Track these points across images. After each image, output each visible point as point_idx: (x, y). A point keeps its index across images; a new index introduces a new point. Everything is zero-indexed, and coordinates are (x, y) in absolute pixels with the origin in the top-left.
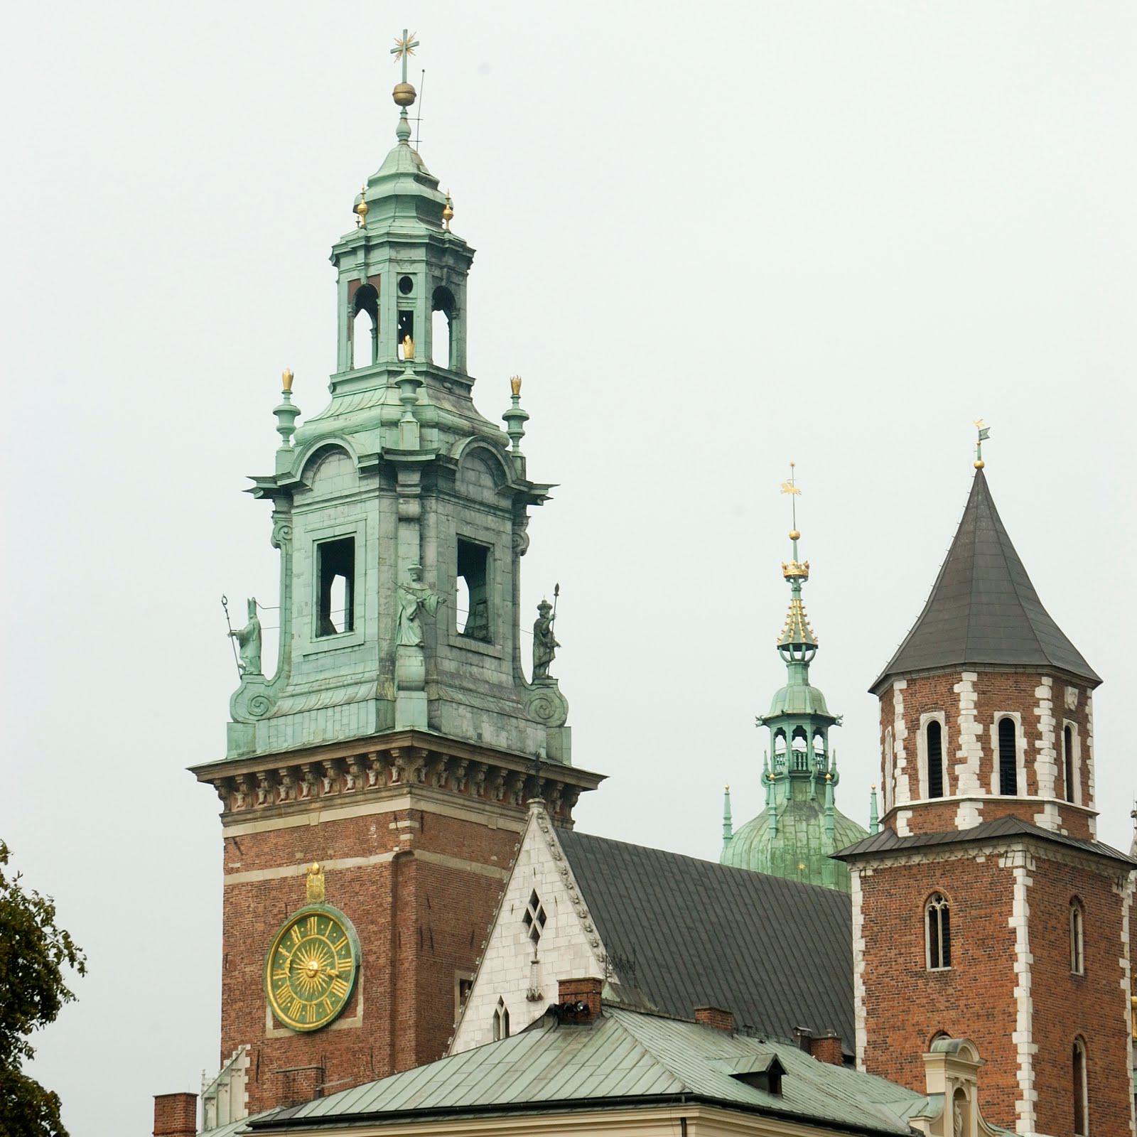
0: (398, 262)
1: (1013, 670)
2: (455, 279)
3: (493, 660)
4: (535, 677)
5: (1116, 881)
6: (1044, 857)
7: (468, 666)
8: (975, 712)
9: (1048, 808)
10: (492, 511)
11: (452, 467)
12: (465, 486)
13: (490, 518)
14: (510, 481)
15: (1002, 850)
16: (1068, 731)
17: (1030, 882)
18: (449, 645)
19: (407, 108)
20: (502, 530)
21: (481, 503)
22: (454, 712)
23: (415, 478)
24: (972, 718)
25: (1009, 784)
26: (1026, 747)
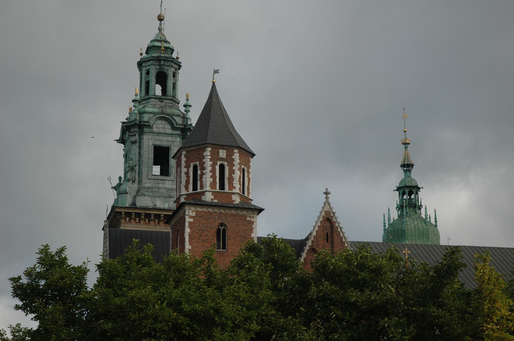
0: (145, 66)
1: (196, 148)
2: (165, 67)
3: (170, 181)
5: (250, 215)
7: (158, 185)
8: (185, 165)
9: (205, 193)
10: (170, 135)
11: (147, 124)
12: (158, 129)
13: (169, 138)
14: (175, 125)
16: (222, 167)
17: (191, 220)
19: (162, 22)
20: (175, 140)
21: (166, 134)
24: (184, 167)
25: (195, 188)
26: (200, 173)
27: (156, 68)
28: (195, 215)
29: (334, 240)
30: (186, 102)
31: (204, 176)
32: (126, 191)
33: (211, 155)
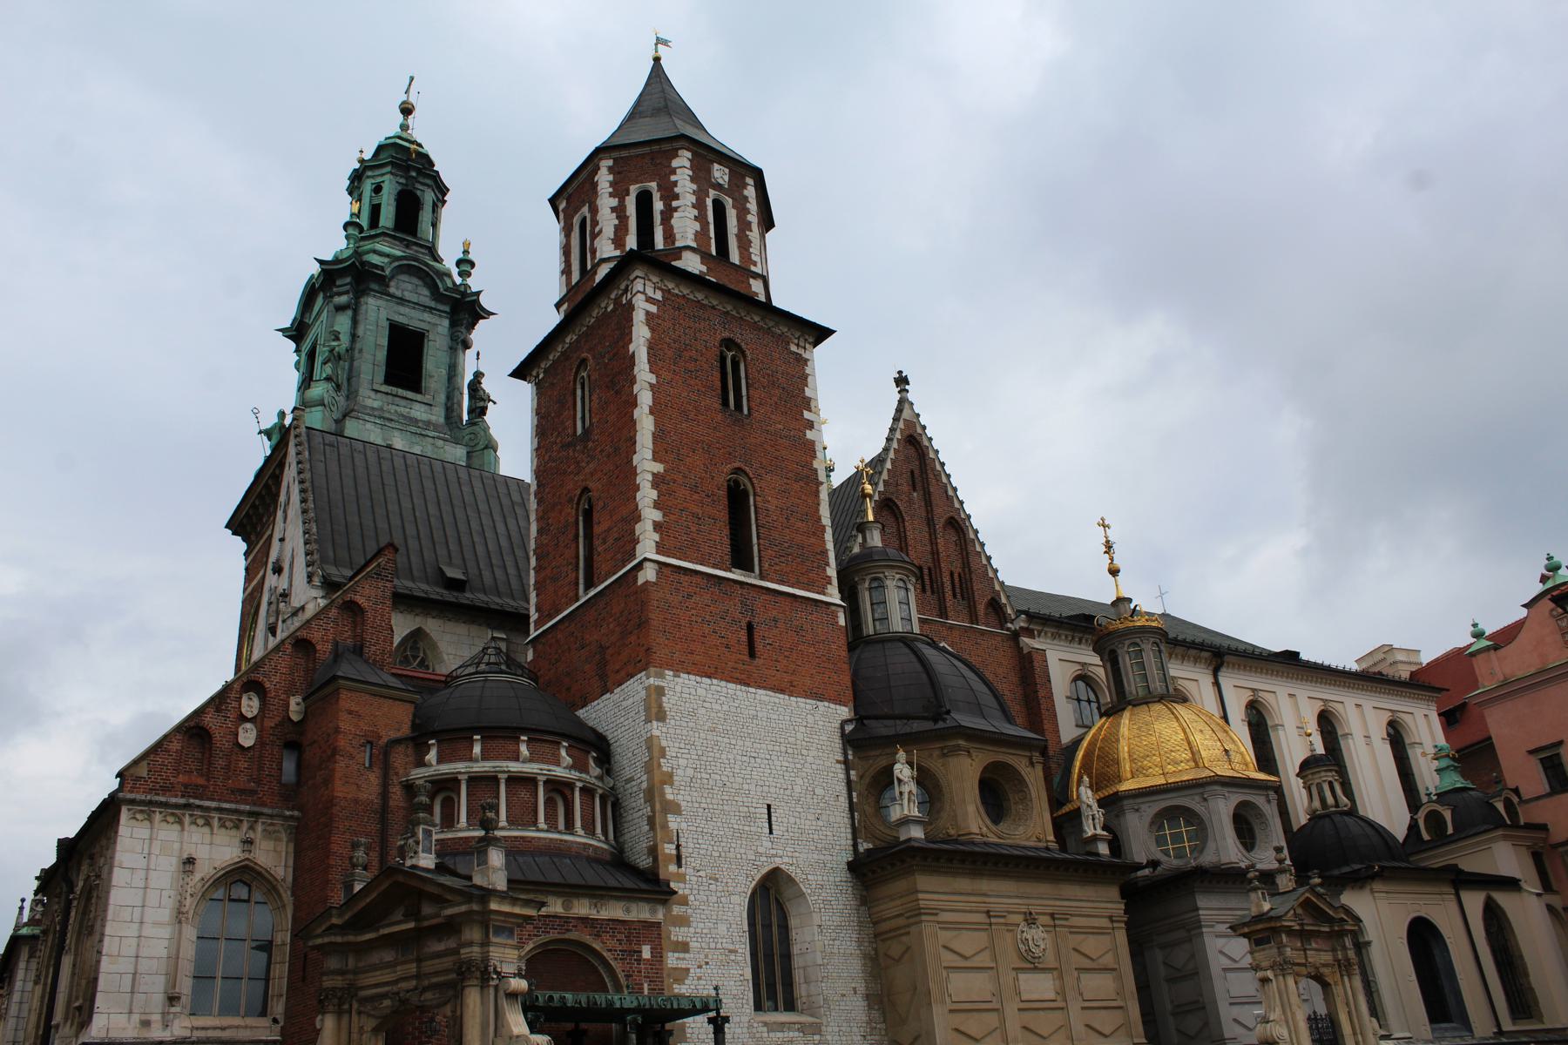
0: (373, 177)
1: (647, 149)
3: (423, 405)
4: (471, 423)
6: (676, 291)
7: (394, 407)
8: (611, 190)
9: (687, 255)
11: (379, 272)
14: (441, 290)
15: (623, 287)
18: (373, 390)
22: (360, 426)
23: (348, 280)
24: (607, 195)
26: (662, 208)
27: (397, 182)
28: (661, 299)
29: (932, 490)
30: (462, 256)
31: (676, 214)
32: (323, 400)
33: (692, 168)
